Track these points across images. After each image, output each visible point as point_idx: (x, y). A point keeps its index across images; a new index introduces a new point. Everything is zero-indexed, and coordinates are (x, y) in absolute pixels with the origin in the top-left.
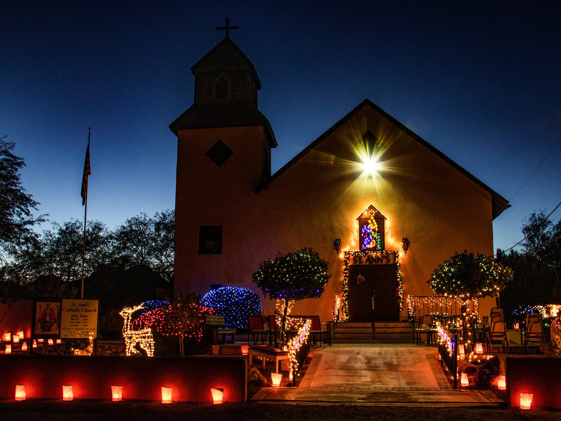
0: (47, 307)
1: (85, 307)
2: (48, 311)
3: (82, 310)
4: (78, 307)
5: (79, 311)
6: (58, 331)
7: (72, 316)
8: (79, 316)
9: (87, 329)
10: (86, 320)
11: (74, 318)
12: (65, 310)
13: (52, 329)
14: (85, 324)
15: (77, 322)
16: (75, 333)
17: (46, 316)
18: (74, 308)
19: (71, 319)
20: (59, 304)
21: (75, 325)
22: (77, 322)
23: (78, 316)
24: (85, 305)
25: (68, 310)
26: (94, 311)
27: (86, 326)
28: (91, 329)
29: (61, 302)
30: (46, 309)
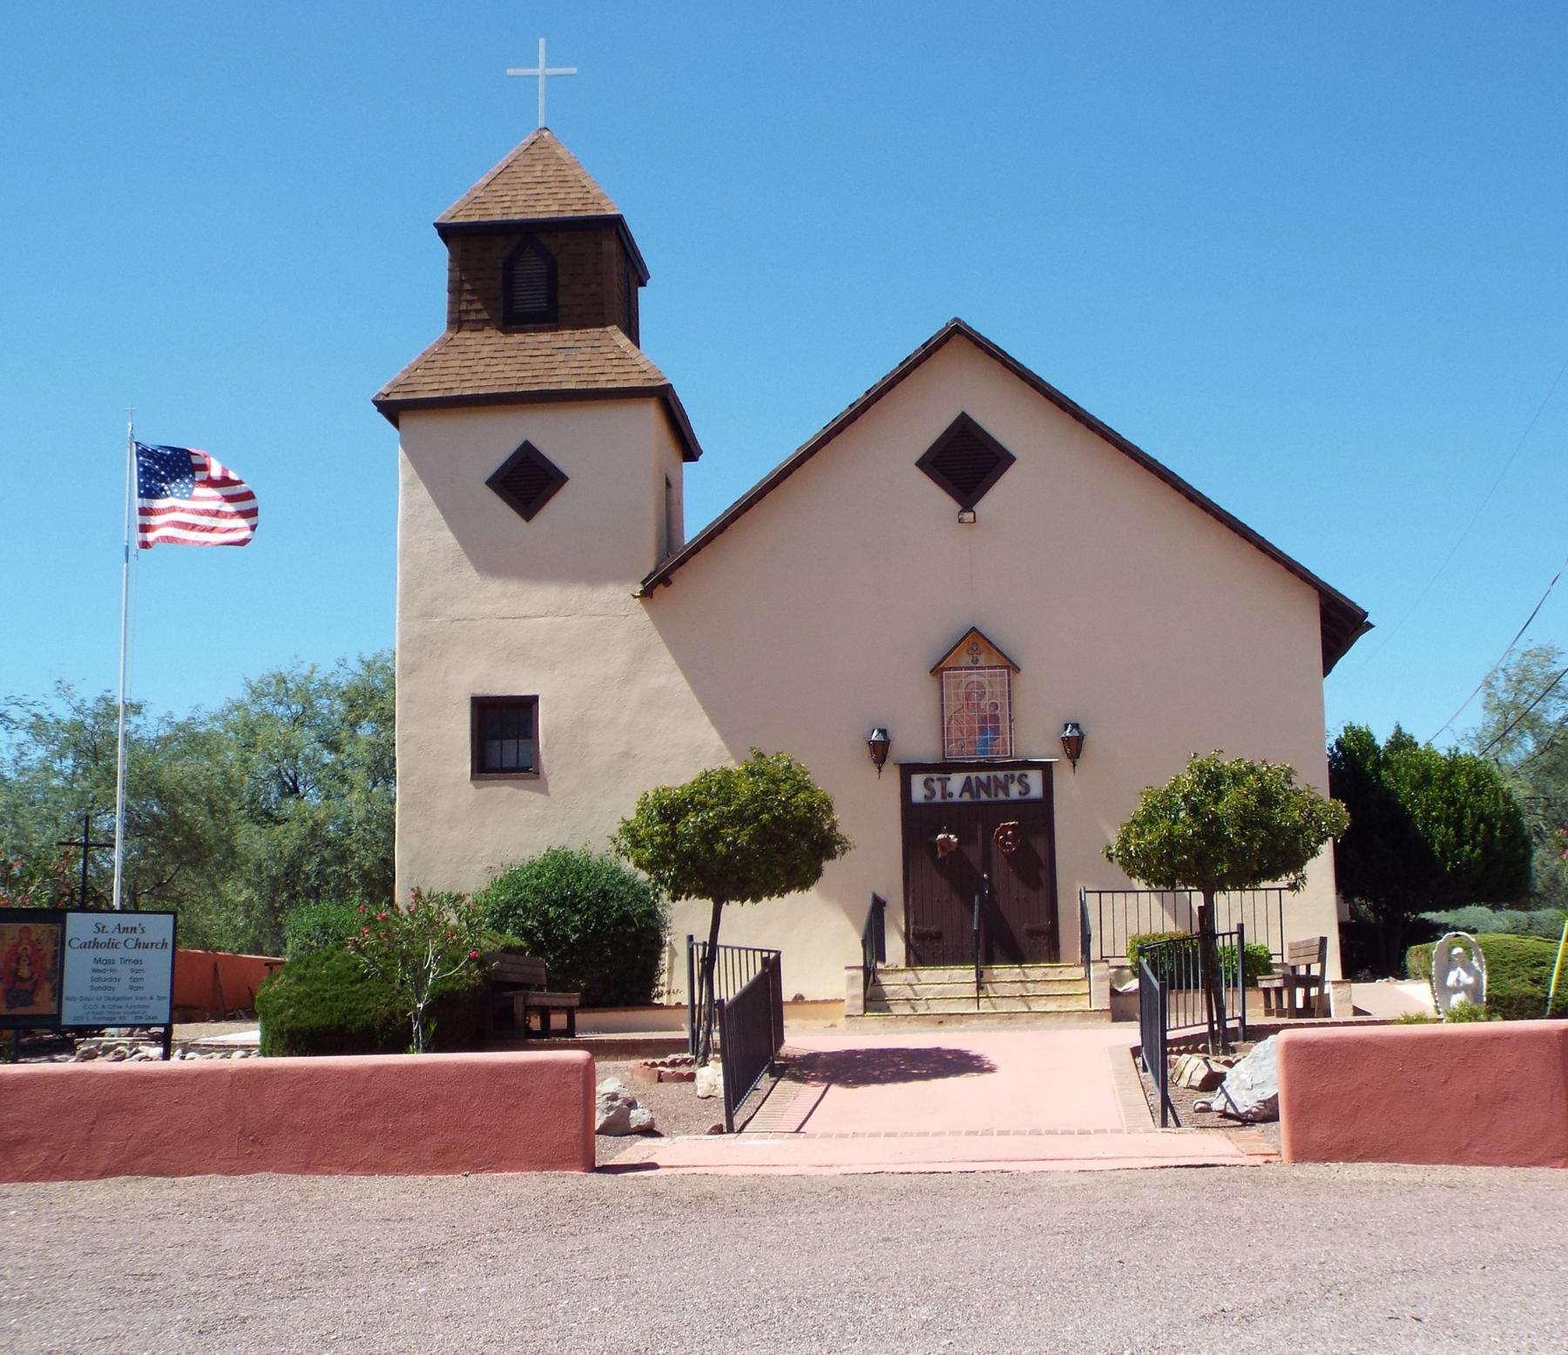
0: (21, 938)
1: (133, 936)
2: (25, 949)
3: (125, 941)
4: (113, 936)
5: (115, 946)
6: (54, 1005)
7: (97, 961)
8: (118, 961)
9: (142, 998)
10: (138, 971)
11: (101, 967)
12: (75, 943)
13: (38, 999)
14: (138, 976)
15: (111, 980)
16: (104, 1010)
17: (18, 962)
18: (102, 938)
19: (94, 970)
20: (56, 928)
21: (106, 988)
22: (111, 980)
23: (113, 962)
24: (134, 930)
25: (84, 946)
26: (160, 946)
27: (138, 988)
28: (151, 998)
29: (63, 923)
30: (19, 944)
